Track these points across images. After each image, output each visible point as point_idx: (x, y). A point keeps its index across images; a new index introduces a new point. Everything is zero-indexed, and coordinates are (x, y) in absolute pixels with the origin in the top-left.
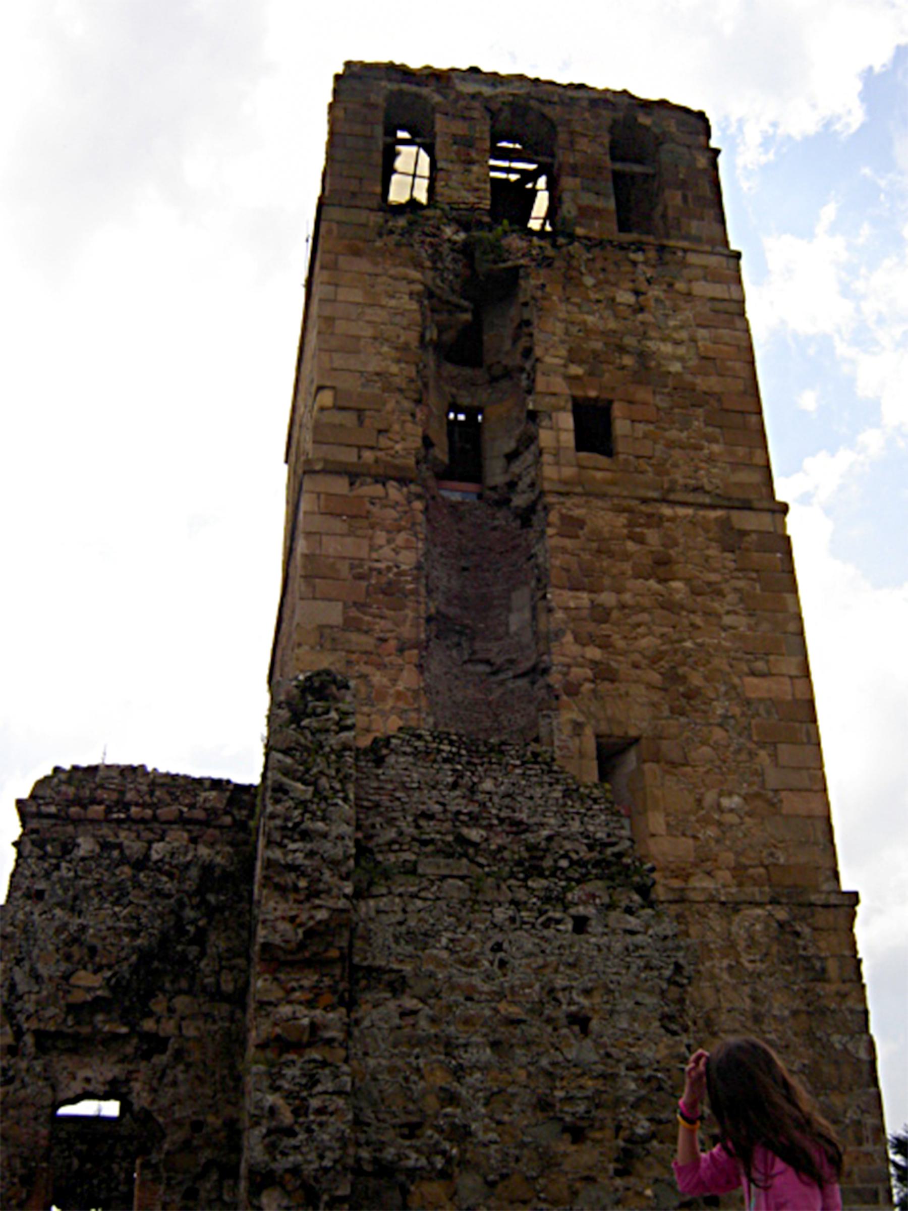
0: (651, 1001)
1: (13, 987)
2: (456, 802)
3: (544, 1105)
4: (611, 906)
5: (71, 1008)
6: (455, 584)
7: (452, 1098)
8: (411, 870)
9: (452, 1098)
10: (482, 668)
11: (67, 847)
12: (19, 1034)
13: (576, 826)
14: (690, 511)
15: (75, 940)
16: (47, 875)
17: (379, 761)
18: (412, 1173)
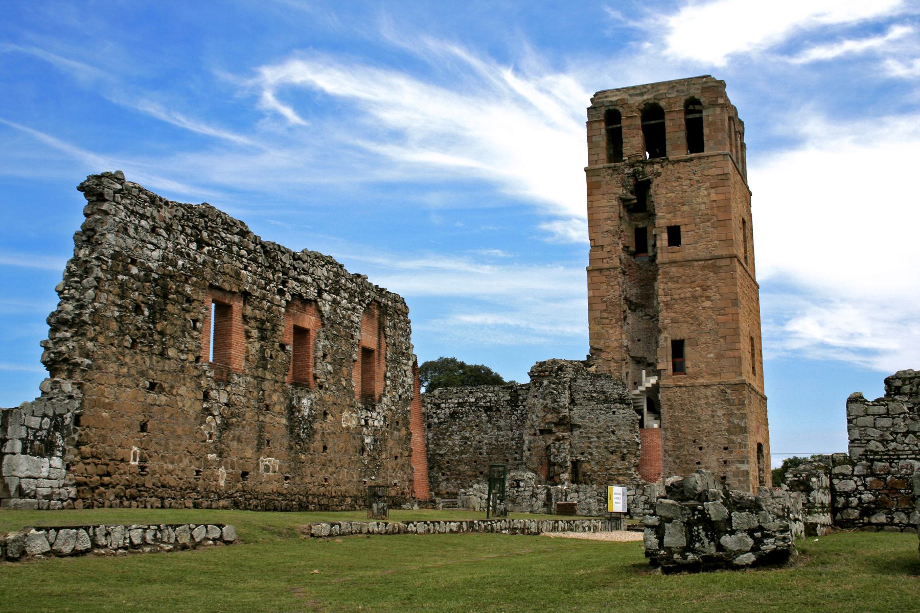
0: (628, 427)
1: (533, 420)
2: (591, 388)
3: (606, 448)
4: (620, 409)
5: (546, 423)
6: (639, 292)
7: (589, 447)
8: (581, 404)
9: (589, 447)
10: (648, 317)
11: (541, 384)
12: (536, 430)
13: (616, 391)
14: (703, 262)
15: (545, 407)
16: (537, 391)
17: (576, 381)
18: (583, 461)
